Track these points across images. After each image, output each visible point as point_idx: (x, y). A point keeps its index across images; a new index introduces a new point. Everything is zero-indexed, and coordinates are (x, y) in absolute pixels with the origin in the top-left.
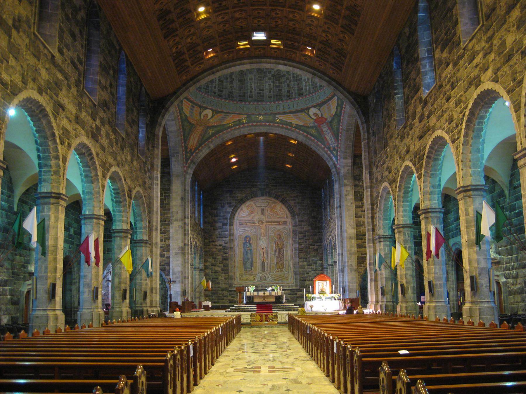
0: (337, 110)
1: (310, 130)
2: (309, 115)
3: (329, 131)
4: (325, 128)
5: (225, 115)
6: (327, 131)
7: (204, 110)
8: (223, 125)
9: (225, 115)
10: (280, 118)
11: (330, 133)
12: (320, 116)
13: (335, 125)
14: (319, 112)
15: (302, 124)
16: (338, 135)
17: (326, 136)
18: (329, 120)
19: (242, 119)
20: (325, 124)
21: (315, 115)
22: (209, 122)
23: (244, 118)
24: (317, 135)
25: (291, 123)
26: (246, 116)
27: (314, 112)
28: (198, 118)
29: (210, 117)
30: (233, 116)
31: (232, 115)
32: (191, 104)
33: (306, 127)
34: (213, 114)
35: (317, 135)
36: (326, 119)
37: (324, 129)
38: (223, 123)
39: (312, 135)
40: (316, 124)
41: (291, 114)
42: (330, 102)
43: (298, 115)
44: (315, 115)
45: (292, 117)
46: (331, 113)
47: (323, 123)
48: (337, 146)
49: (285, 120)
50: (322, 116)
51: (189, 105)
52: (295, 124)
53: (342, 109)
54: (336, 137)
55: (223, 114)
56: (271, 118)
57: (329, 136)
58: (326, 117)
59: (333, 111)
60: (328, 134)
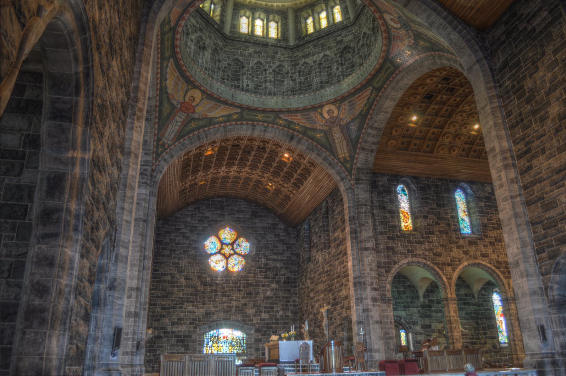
0: (219, 118)
1: (166, 105)
2: (187, 92)
3: (179, 124)
4: (180, 118)
6: (177, 122)
10: (170, 64)
11: (177, 127)
12: (194, 104)
13: (193, 125)
14: (198, 100)
15: (170, 91)
16: (184, 136)
17: (170, 126)
18: (196, 116)
20: (186, 114)
21: (191, 98)
24: (164, 116)
25: (166, 80)
27: (195, 96)
33: (168, 98)
35: (164, 116)
36: (194, 112)
37: (177, 118)
39: (160, 112)
40: (179, 106)
41: (178, 73)
42: (223, 106)
43: (179, 80)
44: (191, 98)
45: (174, 76)
46: (208, 114)
47: (185, 113)
48: (169, 146)
49: (168, 70)
52: (166, 86)
53: (225, 122)
54: (180, 136)
56: (167, 54)
57: (172, 129)
58: (196, 111)
59: (211, 115)
60: (175, 126)
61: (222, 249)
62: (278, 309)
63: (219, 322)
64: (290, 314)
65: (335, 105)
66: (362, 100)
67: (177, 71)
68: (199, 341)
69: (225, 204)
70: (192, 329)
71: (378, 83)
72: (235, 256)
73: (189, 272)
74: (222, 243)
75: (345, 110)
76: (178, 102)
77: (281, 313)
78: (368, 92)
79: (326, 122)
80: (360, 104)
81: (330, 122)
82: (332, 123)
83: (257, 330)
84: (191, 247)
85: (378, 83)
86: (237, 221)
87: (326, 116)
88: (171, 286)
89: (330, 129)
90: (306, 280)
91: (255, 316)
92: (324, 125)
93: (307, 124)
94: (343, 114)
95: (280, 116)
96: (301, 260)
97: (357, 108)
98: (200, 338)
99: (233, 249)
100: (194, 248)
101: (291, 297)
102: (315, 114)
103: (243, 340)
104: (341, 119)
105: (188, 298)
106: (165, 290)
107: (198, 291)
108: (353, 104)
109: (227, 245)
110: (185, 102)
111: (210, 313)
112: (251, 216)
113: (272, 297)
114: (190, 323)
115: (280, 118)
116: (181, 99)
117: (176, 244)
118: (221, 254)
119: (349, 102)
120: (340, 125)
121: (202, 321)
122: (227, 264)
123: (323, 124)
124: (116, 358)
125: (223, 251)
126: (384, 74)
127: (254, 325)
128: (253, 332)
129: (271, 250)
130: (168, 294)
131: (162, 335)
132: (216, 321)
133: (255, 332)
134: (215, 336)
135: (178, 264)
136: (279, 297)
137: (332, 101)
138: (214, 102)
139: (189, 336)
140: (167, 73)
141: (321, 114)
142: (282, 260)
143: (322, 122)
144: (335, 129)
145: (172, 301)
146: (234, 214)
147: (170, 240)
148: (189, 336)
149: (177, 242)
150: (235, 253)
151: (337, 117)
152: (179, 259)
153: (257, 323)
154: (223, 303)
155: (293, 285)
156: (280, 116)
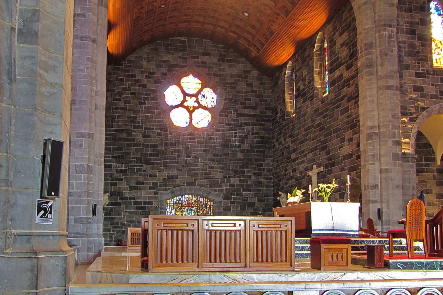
61: (184, 100)
62: (249, 174)
63: (182, 187)
64: (262, 180)
68: (161, 208)
69: (187, 44)
70: (153, 195)
72: (201, 110)
73: (147, 129)
74: (185, 94)
77: (253, 178)
83: (226, 198)
84: (148, 98)
86: (202, 67)
88: (128, 145)
90: (285, 139)
91: (223, 181)
96: (279, 115)
98: (161, 205)
99: (197, 101)
100: (153, 99)
101: (264, 161)
103: (210, 208)
105: (147, 159)
106: (120, 150)
107: (159, 151)
109: (191, 96)
111: (172, 177)
112: (219, 60)
113: (243, 159)
114: (150, 188)
117: (132, 94)
118: (184, 107)
121: (164, 186)
122: (191, 118)
124: (49, 221)
125: (185, 104)
127: (221, 191)
128: (220, 199)
129: (242, 103)
130: (125, 153)
131: (119, 201)
132: (179, 186)
133: (224, 199)
134: (179, 203)
135: (135, 118)
136: (251, 160)
139: (151, 203)
142: (254, 116)
145: (130, 161)
146: (198, 58)
147: (124, 89)
148: (151, 203)
149: (132, 91)
150: (200, 106)
152: (135, 112)
153: (226, 190)
154: (187, 165)
155: (267, 145)
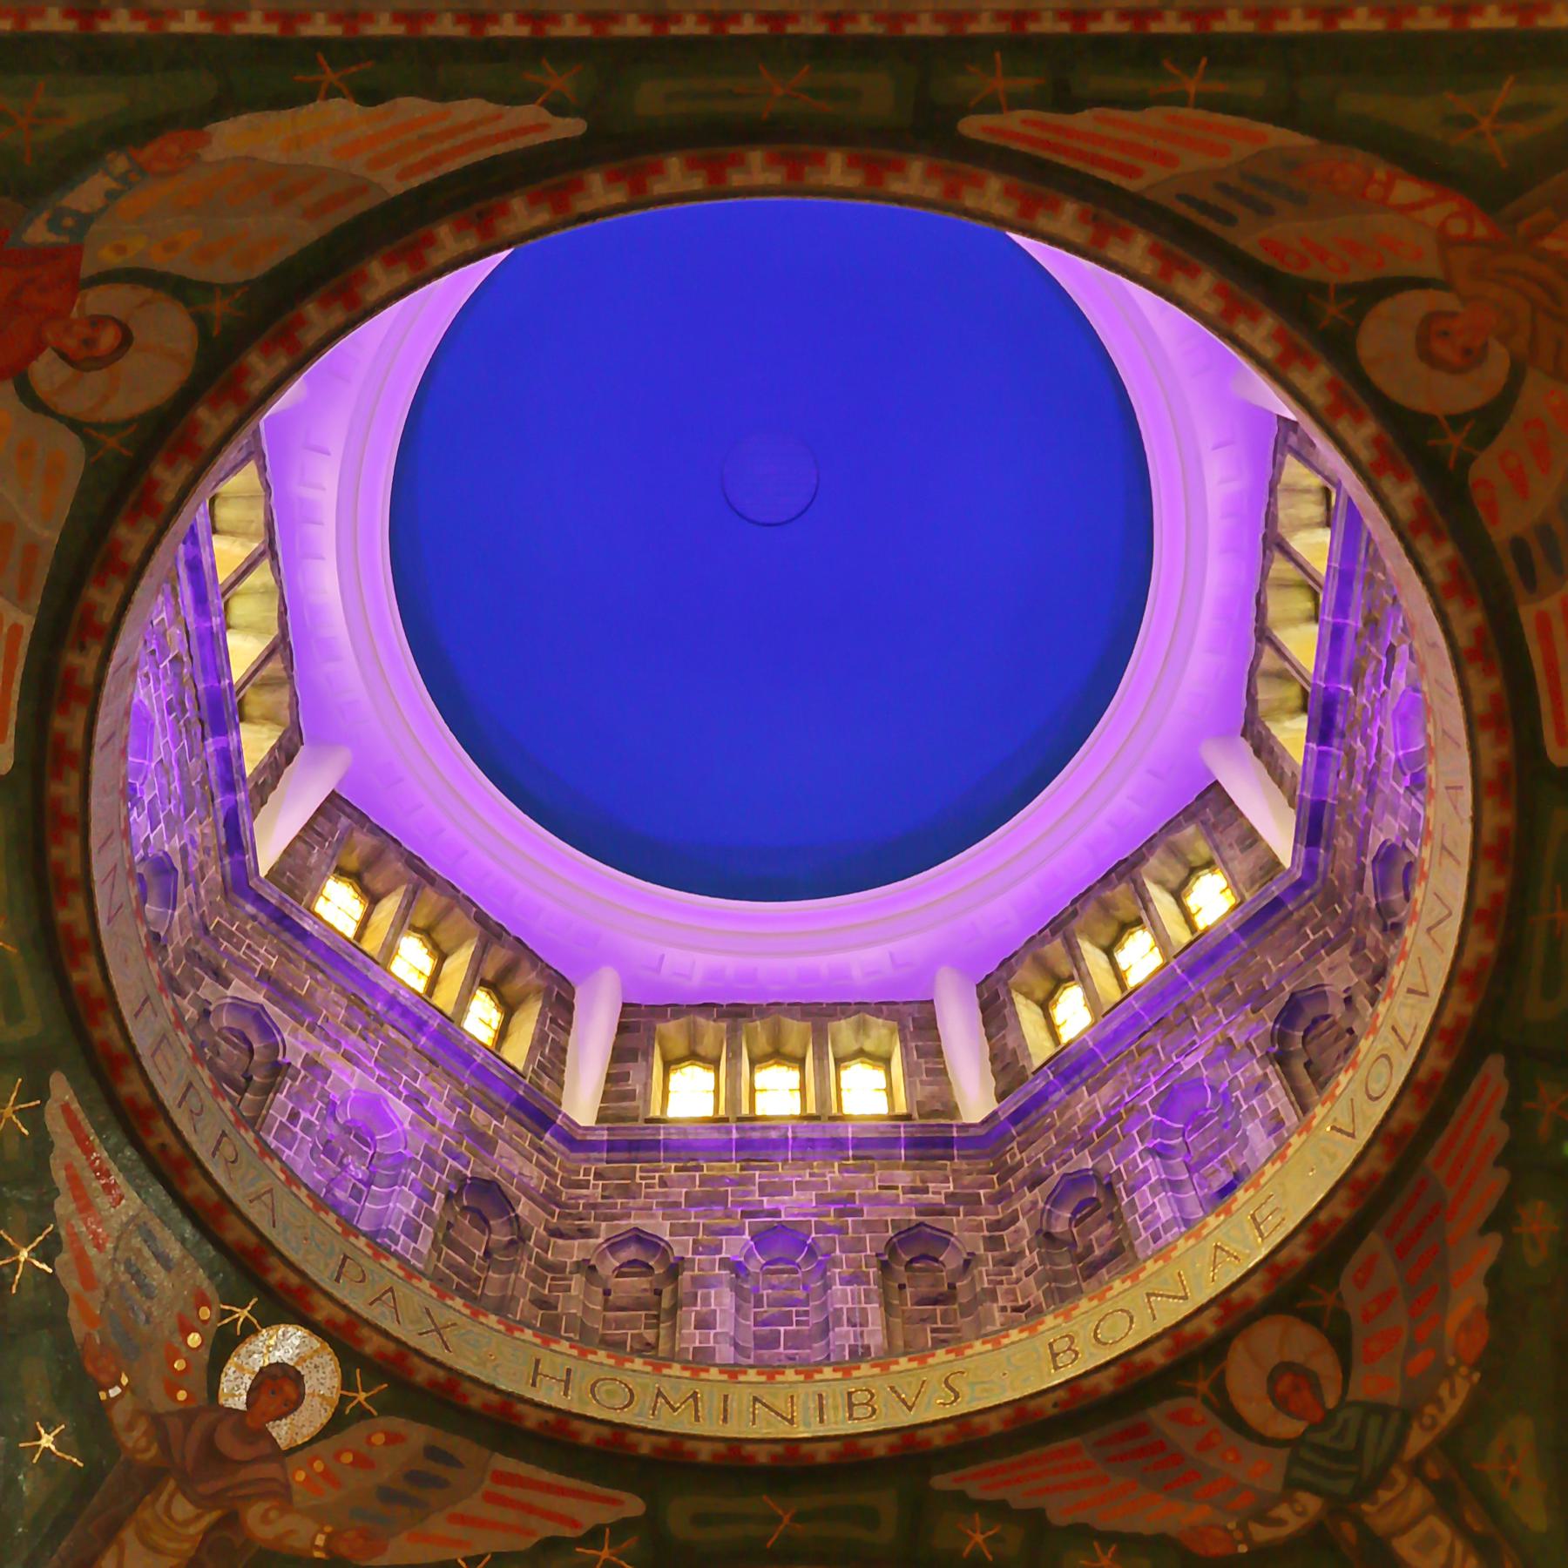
5: (1229, 219)
7: (1425, 421)
8: (1286, 116)
9: (1229, 219)
12: (46, 371)
19: (1018, 102)
21: (108, 338)
22: (1446, 241)
23: (990, 106)
25: (369, 96)
26: (972, 126)
27: (131, 362)
28: (1537, 395)
29: (1416, 304)
30: (1134, 172)
31: (1132, 185)
32: (1527, 614)
34: (1359, 314)
38: (1279, 137)
41: (396, 188)
42: (27, 622)
49: (469, 109)
50: (26, 393)
51: (1544, 623)
52: (306, 96)
55: (1248, 238)
65: (347, 1383)
66: (509, 1516)
67: (416, 182)
71: (700, 1519)
75: (362, 1462)
76: (85, 220)
78: (591, 1514)
79: (188, 1415)
80: (481, 1523)
81: (209, 1443)
82: (211, 1454)
85: (700, 1519)
87: (235, 1389)
89: (152, 1479)
92: (157, 1421)
93: (95, 1301)
94: (326, 1475)
95: (61, 1089)
97: (438, 1525)
102: (202, 1300)
104: (282, 1495)
108: (439, 1483)
110: (75, 284)
115: (36, 1089)
116: (101, 256)
119: (432, 1452)
120: (231, 1520)
123: (161, 1404)
126: (797, 1518)
137: (372, 1345)
138: (50, 536)
140: (443, 94)
141: (225, 1344)
143: (171, 1391)
144: (183, 1508)
151: (282, 1455)
156: (61, 1089)
